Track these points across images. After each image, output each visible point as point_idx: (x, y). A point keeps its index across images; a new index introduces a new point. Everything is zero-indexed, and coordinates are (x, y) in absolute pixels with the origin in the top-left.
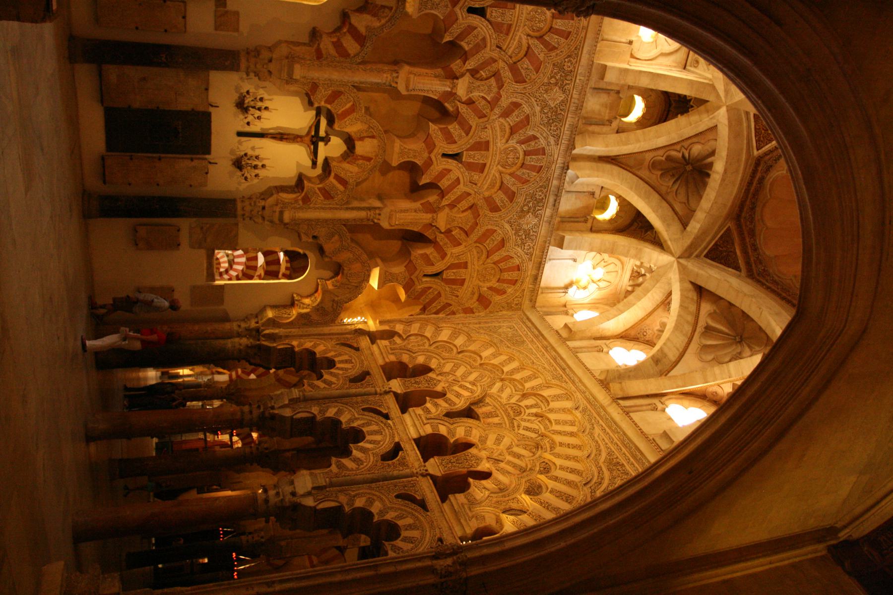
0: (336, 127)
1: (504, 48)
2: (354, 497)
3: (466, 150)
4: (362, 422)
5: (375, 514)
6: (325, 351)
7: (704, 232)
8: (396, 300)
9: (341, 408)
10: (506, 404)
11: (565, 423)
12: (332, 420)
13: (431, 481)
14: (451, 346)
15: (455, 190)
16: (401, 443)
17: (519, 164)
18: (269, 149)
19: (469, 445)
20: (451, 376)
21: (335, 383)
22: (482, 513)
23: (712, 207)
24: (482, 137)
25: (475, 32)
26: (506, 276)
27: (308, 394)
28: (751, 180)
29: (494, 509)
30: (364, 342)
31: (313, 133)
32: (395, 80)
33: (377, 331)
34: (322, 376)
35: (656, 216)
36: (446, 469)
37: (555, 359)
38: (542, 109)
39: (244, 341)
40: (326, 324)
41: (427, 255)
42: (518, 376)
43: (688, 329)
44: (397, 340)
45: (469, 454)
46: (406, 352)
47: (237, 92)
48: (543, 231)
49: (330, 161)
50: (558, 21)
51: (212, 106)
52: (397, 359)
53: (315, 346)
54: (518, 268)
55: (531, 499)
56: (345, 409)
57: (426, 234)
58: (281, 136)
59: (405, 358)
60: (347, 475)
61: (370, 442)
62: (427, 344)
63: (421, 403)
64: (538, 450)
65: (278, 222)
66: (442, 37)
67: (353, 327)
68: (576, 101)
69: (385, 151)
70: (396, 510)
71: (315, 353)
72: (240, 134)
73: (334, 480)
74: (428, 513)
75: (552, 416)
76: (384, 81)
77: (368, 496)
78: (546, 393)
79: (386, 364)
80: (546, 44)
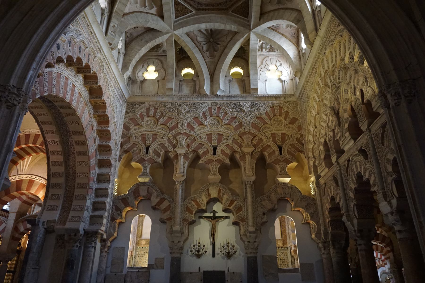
0: (204, 208)
1: (163, 135)
3: (211, 144)
4: (353, 175)
7: (235, 22)
11: (332, 57)
13: (372, 125)
14: (314, 133)
15: (232, 146)
17: (217, 118)
18: (220, 241)
23: (222, 23)
25: (156, 149)
26: (277, 113)
28: (207, 9)
31: (211, 219)
32: (179, 182)
33: (314, 175)
35: (234, 48)
37: (310, 75)
38: (189, 113)
39: (332, 250)
40: (316, 204)
42: (319, 92)
43: (281, 11)
44: (316, 164)
48: (251, 100)
50: (150, 114)
54: (272, 107)
58: (213, 235)
59: (322, 157)
65: (256, 234)
66: (160, 163)
67: (316, 189)
68: (185, 98)
69: (215, 183)
71: (330, 208)
72: (213, 256)
76: (181, 187)
78: (323, 74)
80: (160, 117)
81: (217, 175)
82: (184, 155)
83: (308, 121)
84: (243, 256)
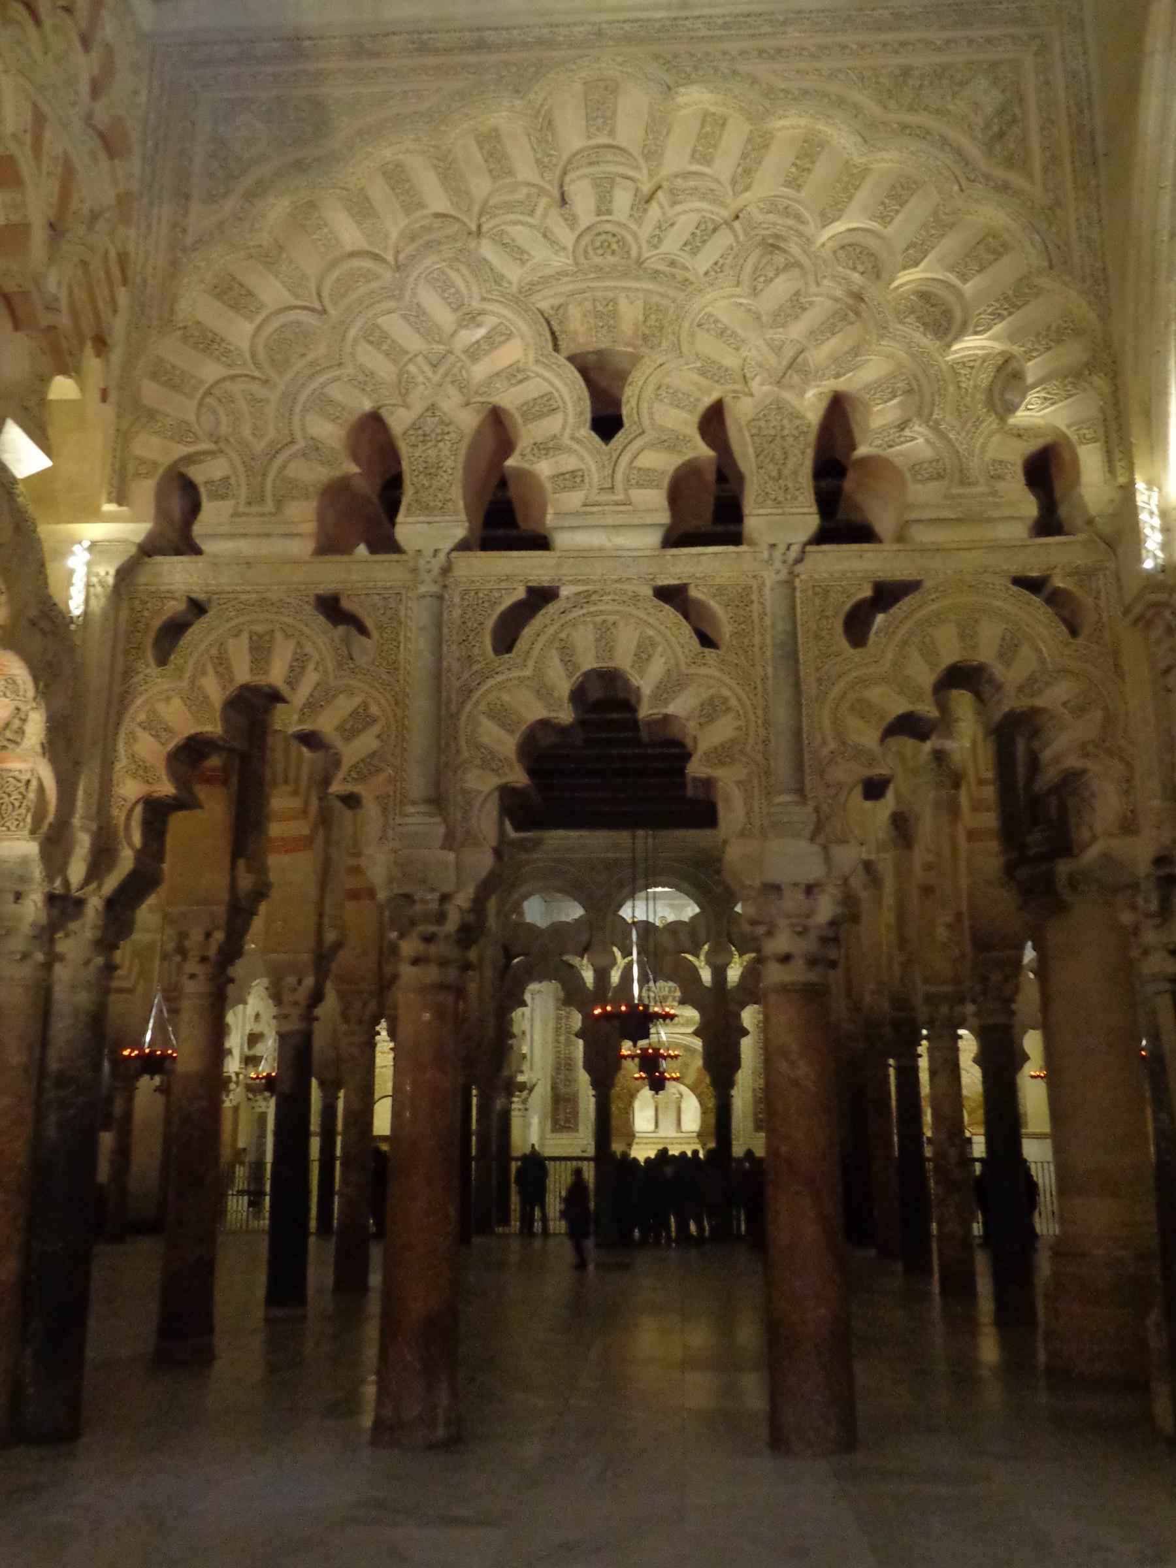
2: (844, 743)
9: (483, 707)
20: (412, 368)
21: (365, 705)
52: (307, 496)
56: (490, 697)
60: (760, 747)
61: (643, 655)
64: (785, 251)
74: (928, 584)
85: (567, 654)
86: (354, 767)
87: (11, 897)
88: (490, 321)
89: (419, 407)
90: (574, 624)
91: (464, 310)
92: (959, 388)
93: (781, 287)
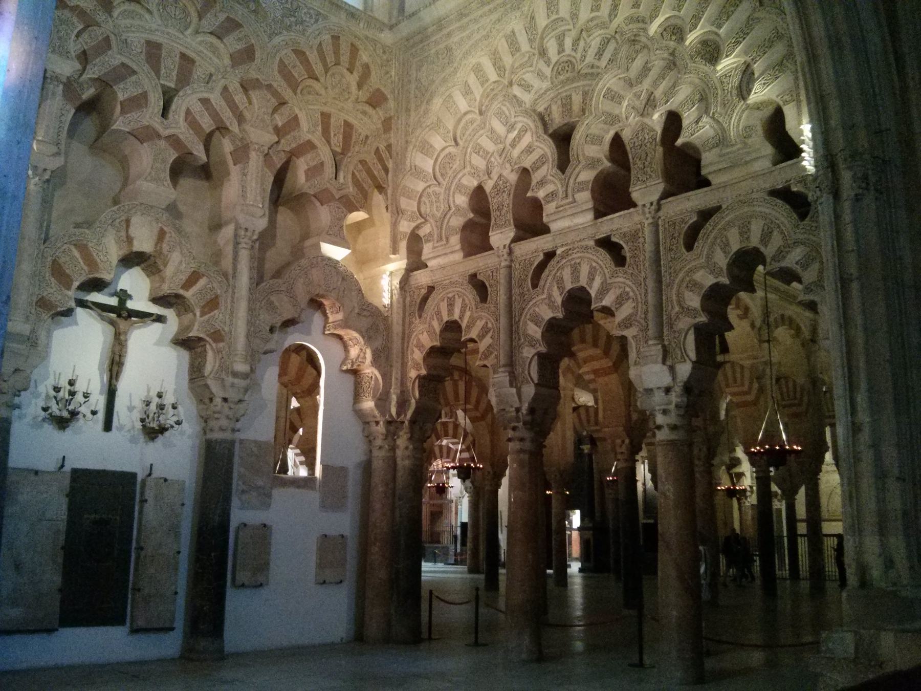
0: (107, 277)
2: (683, 308)
3: (159, 79)
4: (555, 288)
5: (715, 281)
6: (431, 332)
8: (359, 227)
10: (552, 83)
12: (546, 330)
14: (442, 156)
16: (597, 238)
19: (617, 141)
20: (493, 159)
21: (486, 323)
22: (740, 128)
24: (140, 50)
26: (345, 58)
27: (503, 360)
29: (736, 111)
30: (422, 278)
31: (113, 316)
33: (408, 258)
34: (472, 340)
36: (654, 176)
40: (388, 328)
41: (309, 169)
45: (632, 141)
46: (446, 220)
47: (41, 427)
49: (161, 294)
51: (62, 466)
53: (420, 346)
54: (336, 38)
55: (727, 56)
56: (531, 311)
57: (279, 166)
59: (457, 222)
60: (643, 316)
61: (591, 279)
62: (437, 189)
63: (537, 206)
64: (640, 41)
65: (248, 381)
69: (152, 207)
70: (711, 252)
71: (432, 348)
72: (108, 426)
73: (651, 332)
74: (724, 206)
75: (584, 15)
77: (683, 288)
79: (463, 249)
81: (165, 183)
82: (65, 85)
83: (431, 119)
84: (189, 437)
85: (560, 282)
86: (483, 352)
87: (374, 424)
88: (519, 126)
89: (495, 176)
90: (562, 268)
91: (508, 124)
92: (724, 90)
93: (638, 63)
